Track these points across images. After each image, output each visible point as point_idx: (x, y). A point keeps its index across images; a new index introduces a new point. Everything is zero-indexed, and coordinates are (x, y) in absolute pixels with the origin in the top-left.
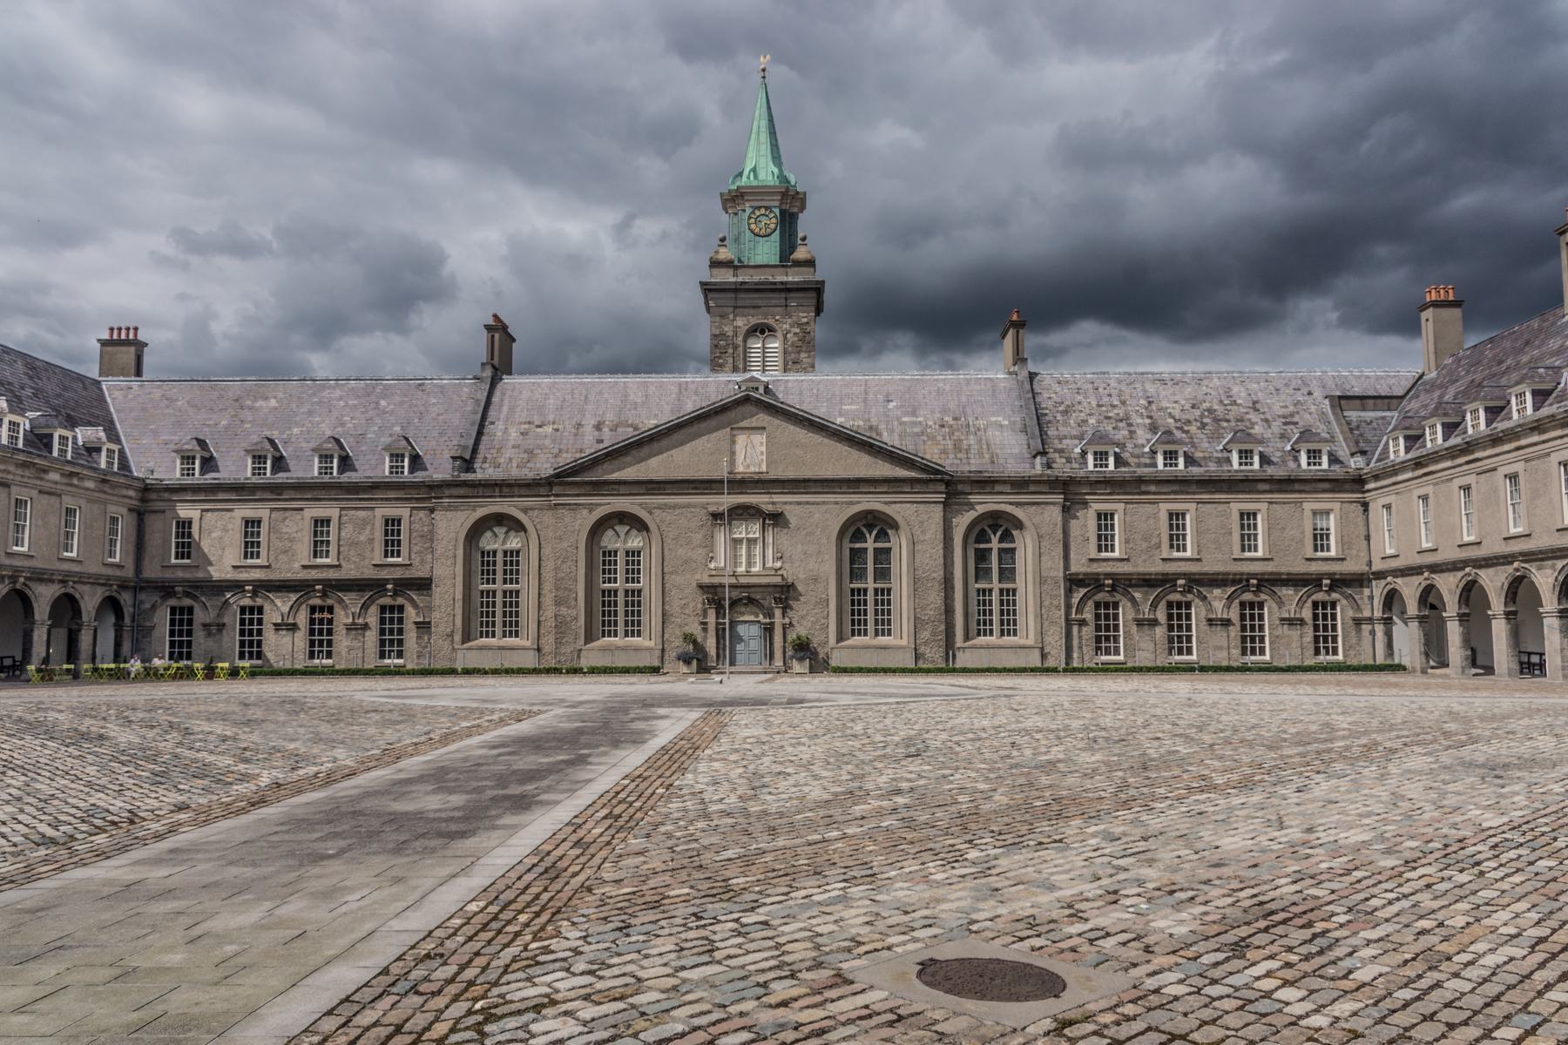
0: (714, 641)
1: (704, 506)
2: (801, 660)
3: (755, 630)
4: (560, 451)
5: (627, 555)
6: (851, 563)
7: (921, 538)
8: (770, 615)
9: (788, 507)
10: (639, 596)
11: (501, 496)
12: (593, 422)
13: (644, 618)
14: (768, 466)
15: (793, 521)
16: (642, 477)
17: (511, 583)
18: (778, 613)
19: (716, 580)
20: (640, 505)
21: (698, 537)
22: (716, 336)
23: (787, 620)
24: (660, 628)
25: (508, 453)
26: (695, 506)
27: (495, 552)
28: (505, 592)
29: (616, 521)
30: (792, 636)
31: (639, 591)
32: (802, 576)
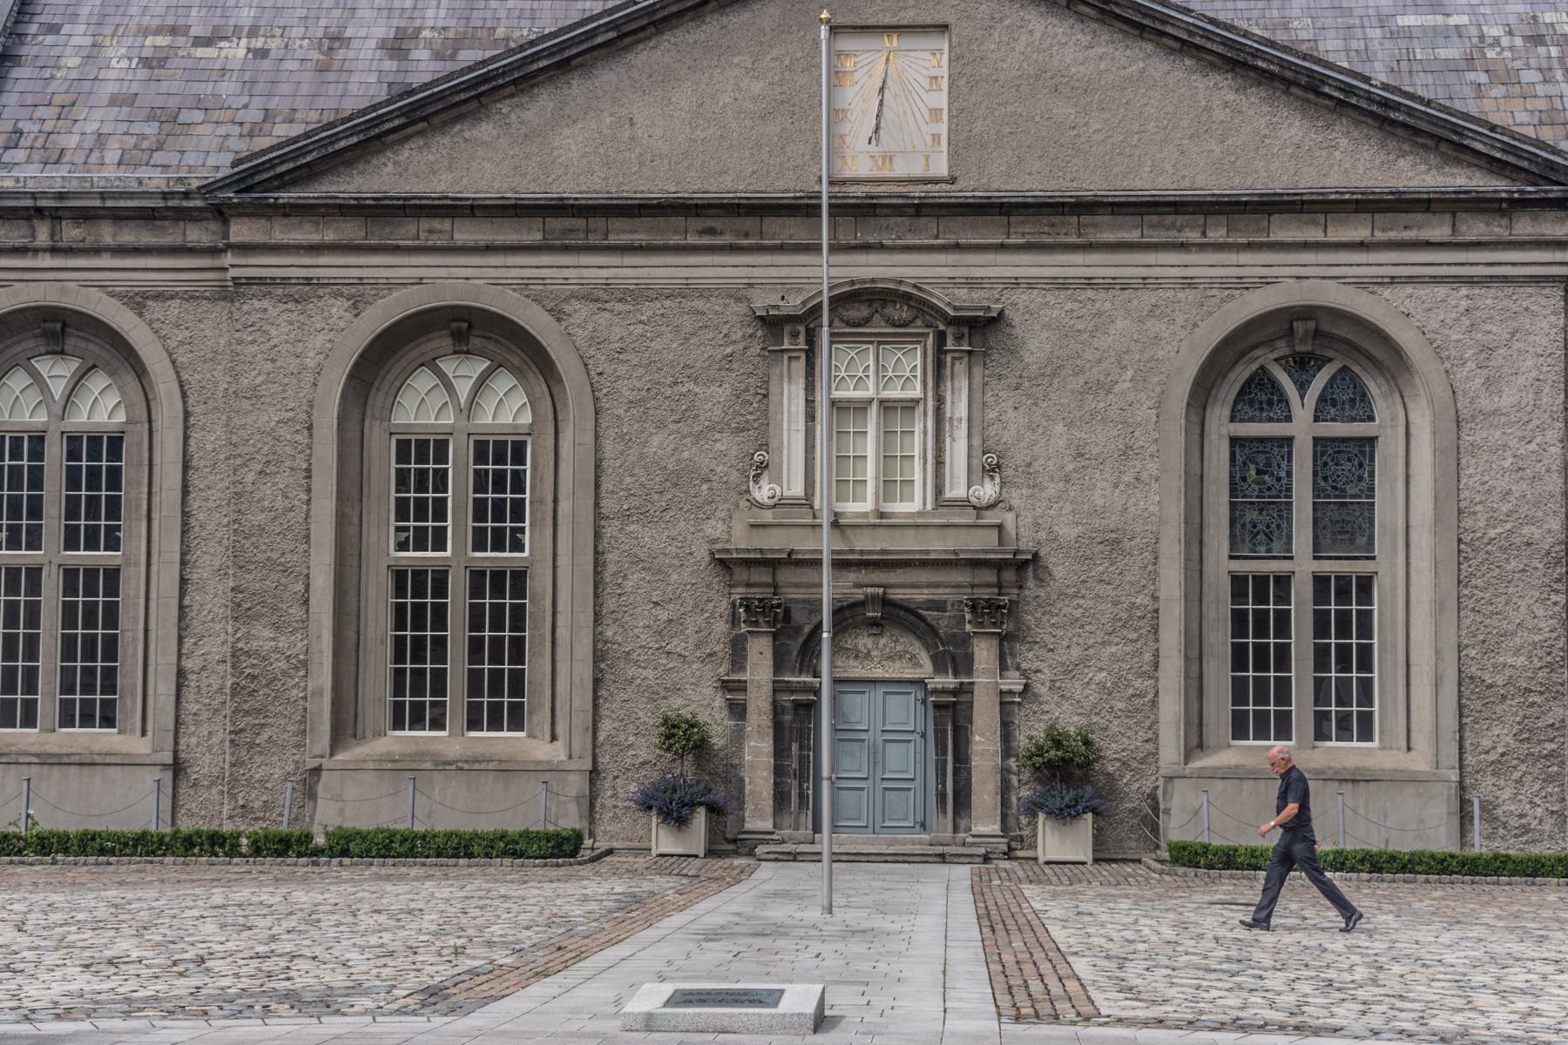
0: (767, 746)
1: (738, 293)
2: (1065, 814)
3: (905, 712)
4: (268, 115)
5: (480, 456)
6: (1233, 491)
7: (1485, 403)
8: (960, 662)
9: (1021, 297)
10: (519, 591)
11: (54, 251)
12: (381, 31)
13: (535, 667)
14: (954, 155)
15: (1036, 345)
16: (530, 188)
17: (92, 544)
18: (984, 653)
19: (776, 542)
20: (524, 286)
21: (715, 397)
23: (1013, 682)
24: (583, 700)
25: (93, 121)
26: (704, 293)
27: (38, 441)
28: (70, 574)
29: (445, 343)
30: (1031, 731)
31: (520, 577)
32: (1067, 532)
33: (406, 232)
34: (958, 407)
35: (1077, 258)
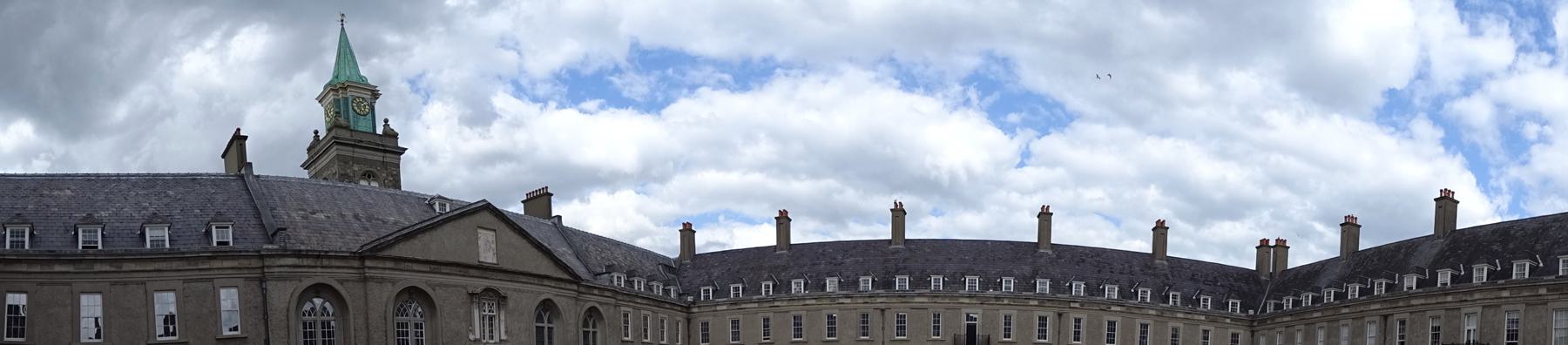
15: (511, 304)
22: (342, 175)
33: (403, 265)
34: (502, 318)
35: (518, 284)
